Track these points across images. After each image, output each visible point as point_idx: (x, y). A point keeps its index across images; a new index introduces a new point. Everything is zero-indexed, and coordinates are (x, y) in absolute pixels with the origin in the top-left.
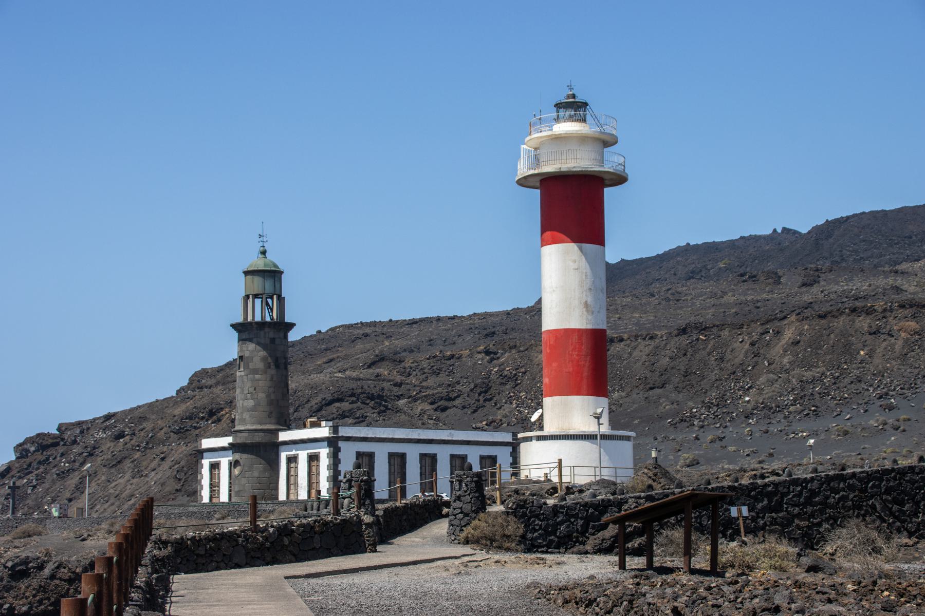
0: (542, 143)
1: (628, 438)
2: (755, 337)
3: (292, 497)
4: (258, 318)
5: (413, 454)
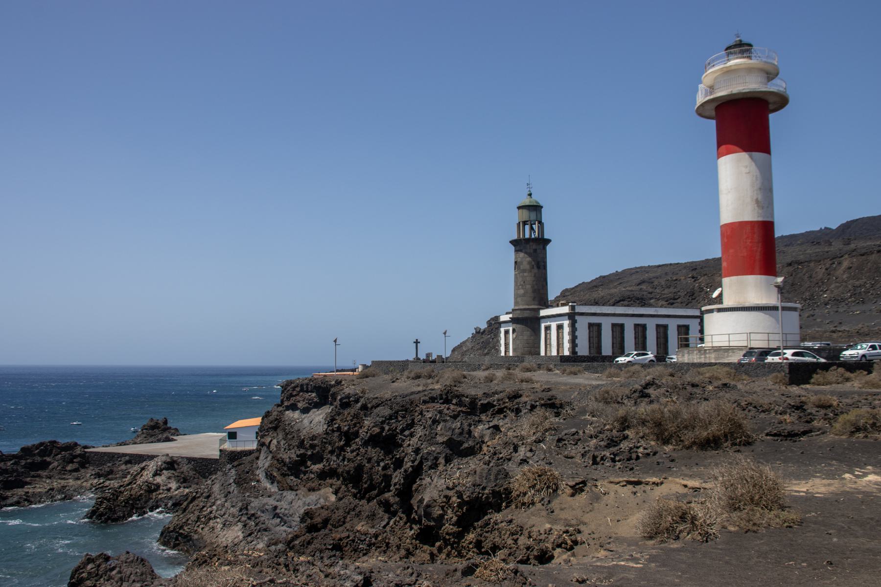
0: (716, 78)
1: (795, 309)
2: (828, 266)
3: (548, 354)
4: (527, 236)
5: (629, 326)
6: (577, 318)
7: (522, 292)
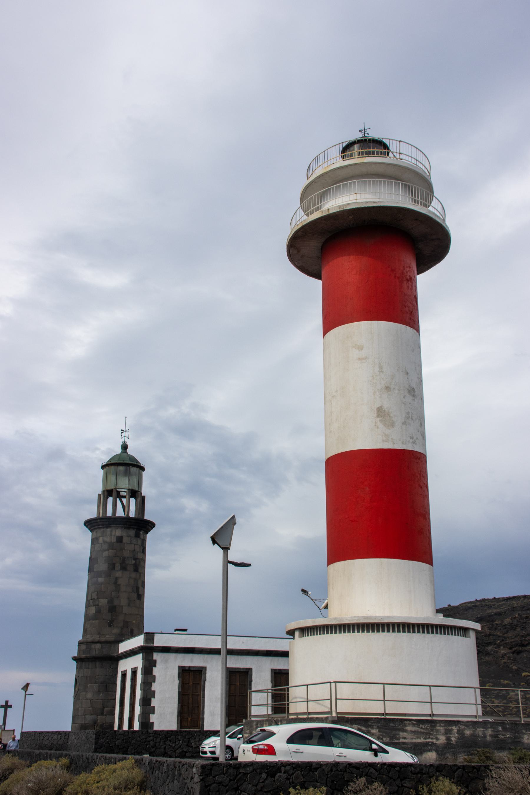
1: (464, 631)
4: (109, 513)
6: (156, 656)
7: (93, 610)
